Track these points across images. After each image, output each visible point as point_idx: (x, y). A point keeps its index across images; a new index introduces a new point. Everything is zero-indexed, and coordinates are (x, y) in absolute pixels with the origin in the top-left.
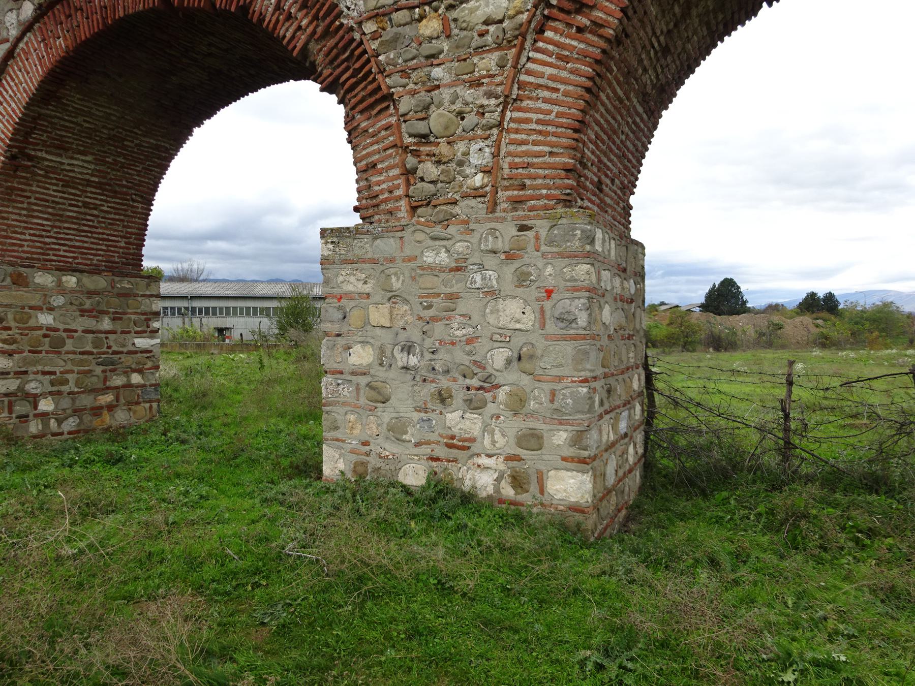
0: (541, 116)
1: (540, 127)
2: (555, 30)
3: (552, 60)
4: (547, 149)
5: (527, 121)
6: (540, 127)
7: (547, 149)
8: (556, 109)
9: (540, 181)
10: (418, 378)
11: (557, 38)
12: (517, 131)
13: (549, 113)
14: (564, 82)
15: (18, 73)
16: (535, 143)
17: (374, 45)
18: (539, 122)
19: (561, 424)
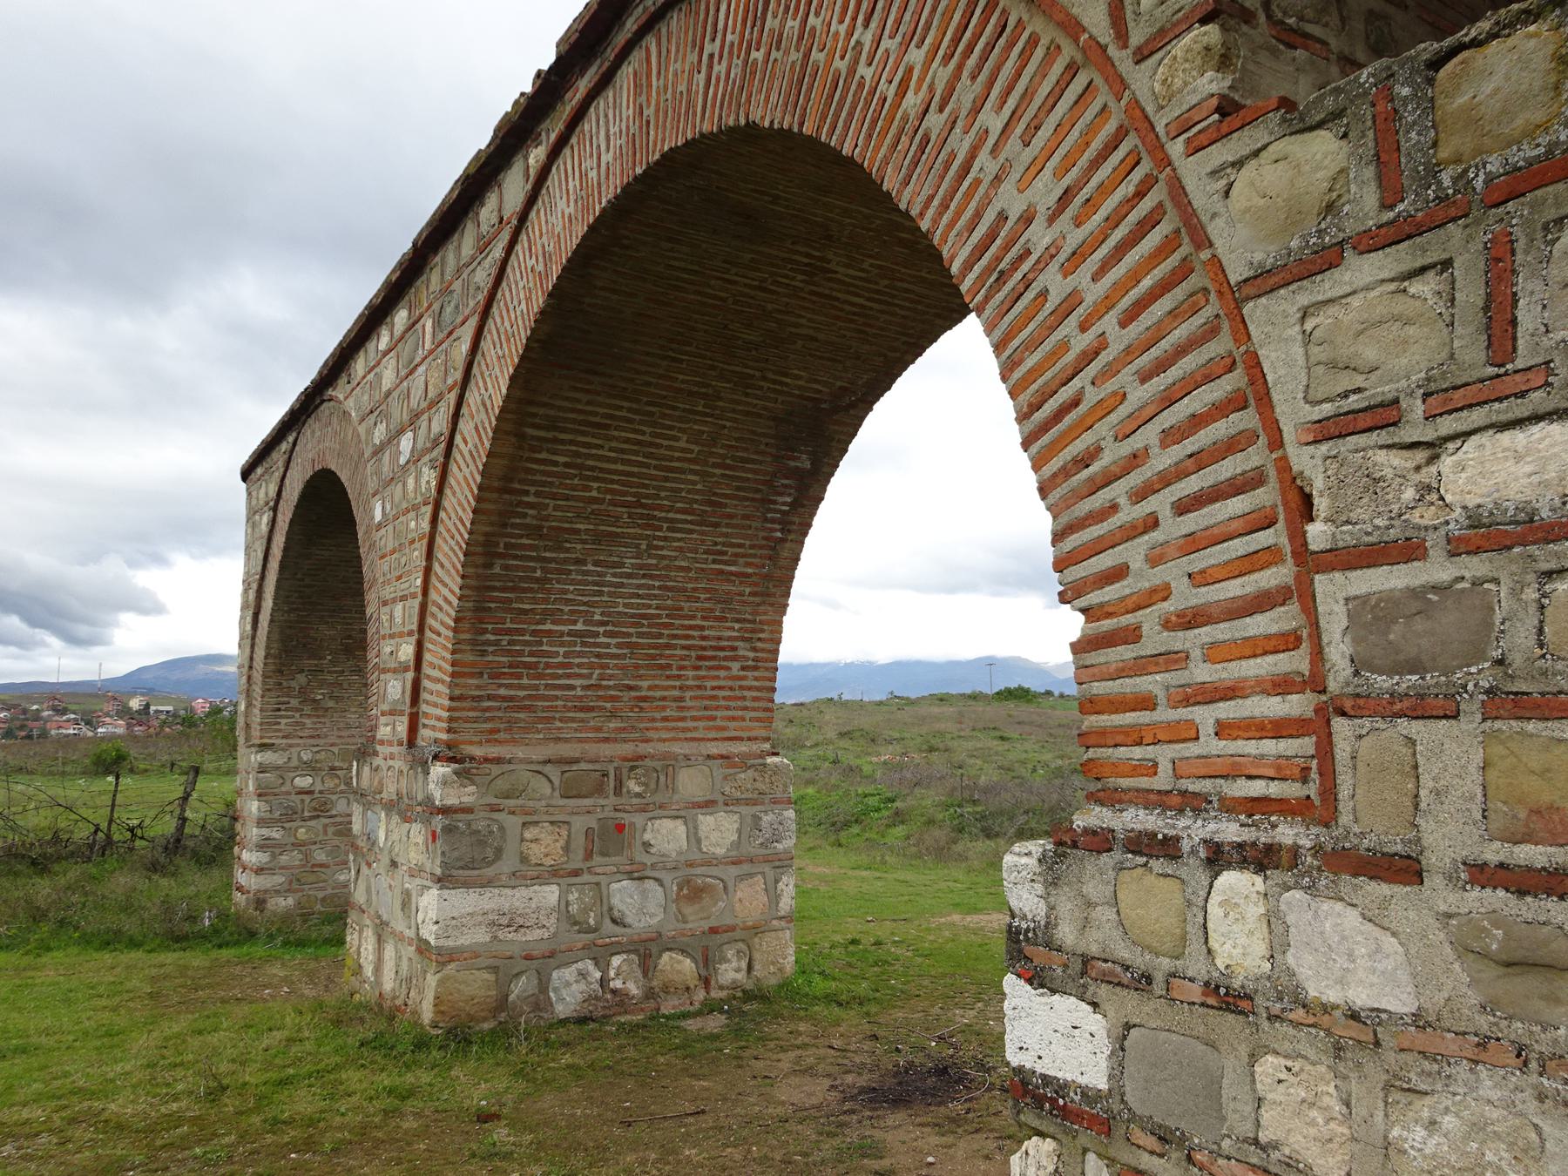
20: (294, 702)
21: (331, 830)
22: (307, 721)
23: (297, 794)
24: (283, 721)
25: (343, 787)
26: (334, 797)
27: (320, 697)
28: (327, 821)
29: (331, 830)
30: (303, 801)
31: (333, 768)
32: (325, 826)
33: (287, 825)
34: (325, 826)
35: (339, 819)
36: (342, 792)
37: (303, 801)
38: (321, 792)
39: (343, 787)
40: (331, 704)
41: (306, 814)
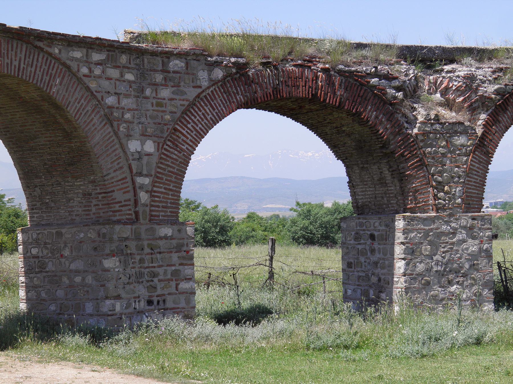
0: (475, 180)
1: (474, 184)
2: (479, 152)
3: (477, 161)
4: (477, 192)
5: (471, 181)
6: (474, 184)
7: (477, 192)
8: (479, 178)
9: (475, 203)
10: (440, 275)
11: (479, 155)
12: (468, 184)
13: (477, 179)
14: (481, 169)
15: (205, 107)
16: (473, 189)
17: (421, 144)
18: (474, 182)
19: (486, 286)
20: (38, 204)
21: (46, 279)
22: (44, 215)
23: (33, 257)
24: (35, 215)
25: (50, 255)
26: (47, 260)
27: (48, 201)
28: (45, 274)
29: (46, 279)
30: (35, 262)
31: (45, 243)
32: (44, 277)
33: (31, 275)
34: (44, 277)
35: (49, 274)
36: (50, 257)
37: (35, 262)
38: (42, 257)
39: (50, 255)
40: (53, 205)
41: (37, 270)
